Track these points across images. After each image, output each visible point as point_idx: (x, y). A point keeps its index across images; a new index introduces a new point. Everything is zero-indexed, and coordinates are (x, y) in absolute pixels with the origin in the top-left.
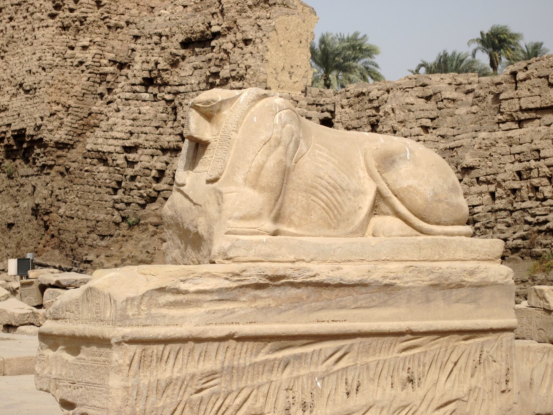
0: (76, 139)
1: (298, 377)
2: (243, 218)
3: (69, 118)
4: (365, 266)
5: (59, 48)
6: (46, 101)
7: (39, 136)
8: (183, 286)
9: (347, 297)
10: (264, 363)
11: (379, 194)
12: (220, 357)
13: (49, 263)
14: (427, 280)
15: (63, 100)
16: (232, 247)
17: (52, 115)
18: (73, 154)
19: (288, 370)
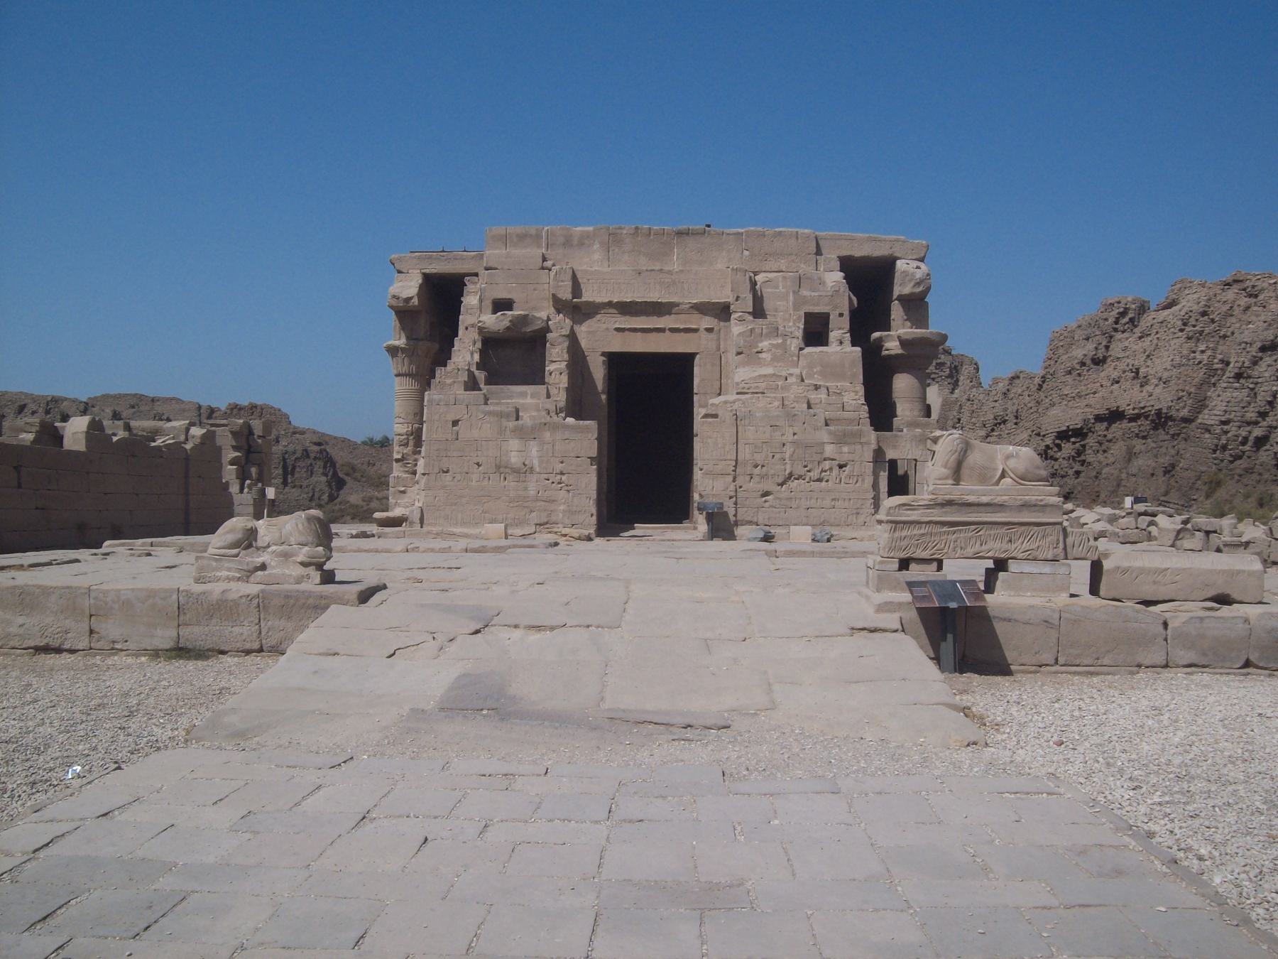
0: (1196, 415)
1: (958, 538)
2: (940, 479)
3: (1191, 401)
4: (992, 497)
5: (1185, 352)
6: (1175, 389)
7: (1170, 414)
8: (913, 503)
9: (983, 509)
10: (945, 532)
11: (1004, 471)
12: (927, 528)
13: (1171, 501)
14: (1020, 503)
15: (1187, 388)
16: (934, 489)
17: (1179, 399)
18: (1193, 425)
19: (955, 535)
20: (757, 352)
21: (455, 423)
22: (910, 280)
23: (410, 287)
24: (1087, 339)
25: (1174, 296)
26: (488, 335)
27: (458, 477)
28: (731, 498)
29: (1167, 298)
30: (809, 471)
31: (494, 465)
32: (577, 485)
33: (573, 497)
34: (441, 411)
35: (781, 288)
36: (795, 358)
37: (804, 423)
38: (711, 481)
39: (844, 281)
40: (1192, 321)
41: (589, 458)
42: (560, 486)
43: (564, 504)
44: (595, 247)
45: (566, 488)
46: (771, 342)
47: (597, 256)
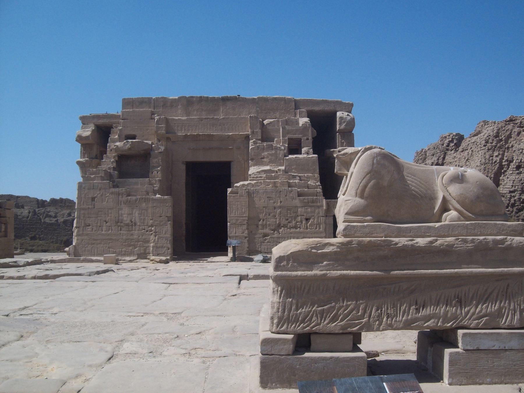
20: (262, 158)
21: (93, 199)
22: (344, 122)
23: (87, 131)
24: (433, 155)
25: (480, 129)
26: (120, 153)
27: (95, 229)
28: (246, 238)
29: (475, 131)
30: (289, 222)
31: (115, 221)
32: (160, 232)
33: (158, 239)
34: (86, 192)
35: (276, 126)
36: (282, 161)
37: (286, 196)
38: (234, 229)
39: (309, 122)
40: (490, 141)
41: (167, 217)
42: (151, 232)
43: (153, 243)
44: (179, 107)
45: (154, 234)
46: (269, 153)
47: (179, 111)
